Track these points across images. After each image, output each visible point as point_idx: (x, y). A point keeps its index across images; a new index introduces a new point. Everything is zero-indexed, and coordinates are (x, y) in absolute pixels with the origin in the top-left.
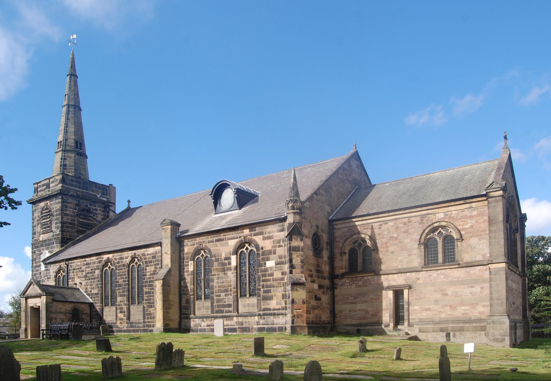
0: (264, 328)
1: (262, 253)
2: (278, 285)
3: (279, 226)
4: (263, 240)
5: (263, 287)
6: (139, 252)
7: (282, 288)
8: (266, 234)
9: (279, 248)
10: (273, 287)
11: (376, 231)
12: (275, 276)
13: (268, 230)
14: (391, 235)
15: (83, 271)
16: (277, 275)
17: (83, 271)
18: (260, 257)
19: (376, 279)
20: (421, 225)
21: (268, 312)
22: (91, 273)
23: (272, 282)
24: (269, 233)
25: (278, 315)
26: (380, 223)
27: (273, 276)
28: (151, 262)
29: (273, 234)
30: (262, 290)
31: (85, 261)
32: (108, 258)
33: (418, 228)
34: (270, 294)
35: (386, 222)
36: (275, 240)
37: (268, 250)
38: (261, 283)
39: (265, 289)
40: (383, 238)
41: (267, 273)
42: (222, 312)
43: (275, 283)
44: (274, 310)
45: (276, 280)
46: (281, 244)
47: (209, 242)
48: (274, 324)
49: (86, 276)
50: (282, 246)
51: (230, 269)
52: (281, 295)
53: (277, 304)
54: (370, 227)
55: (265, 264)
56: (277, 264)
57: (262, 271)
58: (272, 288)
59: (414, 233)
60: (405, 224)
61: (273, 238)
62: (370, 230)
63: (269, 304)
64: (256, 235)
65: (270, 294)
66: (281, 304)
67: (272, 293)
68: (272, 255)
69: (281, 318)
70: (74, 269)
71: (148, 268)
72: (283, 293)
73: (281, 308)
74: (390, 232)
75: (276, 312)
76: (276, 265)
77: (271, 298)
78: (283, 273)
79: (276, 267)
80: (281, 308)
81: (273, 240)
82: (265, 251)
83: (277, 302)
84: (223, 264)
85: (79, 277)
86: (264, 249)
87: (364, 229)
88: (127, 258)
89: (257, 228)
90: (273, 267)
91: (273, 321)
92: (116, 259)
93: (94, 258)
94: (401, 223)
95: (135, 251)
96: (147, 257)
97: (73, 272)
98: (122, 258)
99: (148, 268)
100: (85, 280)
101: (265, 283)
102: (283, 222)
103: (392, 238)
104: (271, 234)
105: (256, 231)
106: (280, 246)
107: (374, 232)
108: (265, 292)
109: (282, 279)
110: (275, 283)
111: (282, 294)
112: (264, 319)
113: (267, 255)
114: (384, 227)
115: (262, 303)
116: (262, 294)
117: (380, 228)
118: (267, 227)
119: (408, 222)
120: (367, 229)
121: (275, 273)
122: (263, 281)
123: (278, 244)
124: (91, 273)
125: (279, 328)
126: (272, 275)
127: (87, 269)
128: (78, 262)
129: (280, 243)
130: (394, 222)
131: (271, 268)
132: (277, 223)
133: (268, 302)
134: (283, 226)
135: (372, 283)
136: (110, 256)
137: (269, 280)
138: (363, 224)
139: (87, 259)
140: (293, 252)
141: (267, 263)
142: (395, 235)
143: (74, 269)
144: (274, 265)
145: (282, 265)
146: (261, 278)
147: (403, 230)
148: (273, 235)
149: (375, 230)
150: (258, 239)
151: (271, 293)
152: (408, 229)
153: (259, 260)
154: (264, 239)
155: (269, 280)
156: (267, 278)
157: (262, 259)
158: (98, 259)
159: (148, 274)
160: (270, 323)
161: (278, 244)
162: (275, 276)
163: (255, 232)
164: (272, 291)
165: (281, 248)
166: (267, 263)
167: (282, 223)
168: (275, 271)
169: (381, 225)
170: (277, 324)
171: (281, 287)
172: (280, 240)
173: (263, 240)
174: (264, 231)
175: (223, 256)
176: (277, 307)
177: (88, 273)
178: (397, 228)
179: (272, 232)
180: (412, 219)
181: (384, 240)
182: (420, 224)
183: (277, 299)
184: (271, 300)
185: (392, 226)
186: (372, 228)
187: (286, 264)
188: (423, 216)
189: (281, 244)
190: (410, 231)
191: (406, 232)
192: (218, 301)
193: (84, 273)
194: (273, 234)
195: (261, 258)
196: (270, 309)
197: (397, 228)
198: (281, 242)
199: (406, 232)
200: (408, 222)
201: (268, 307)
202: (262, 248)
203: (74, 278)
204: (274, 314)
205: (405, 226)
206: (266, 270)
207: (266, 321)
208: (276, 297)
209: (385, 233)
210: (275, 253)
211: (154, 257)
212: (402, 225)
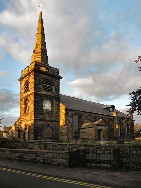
6: (108, 117)
15: (88, 118)
16: (130, 129)
17: (88, 118)
22: (91, 119)
28: (111, 121)
31: (89, 114)
32: (98, 116)
42: (122, 135)
47: (121, 119)
49: (89, 120)
51: (124, 126)
64: (128, 120)
70: (83, 116)
71: (110, 122)
84: (123, 125)
85: (86, 119)
88: (104, 118)
92: (101, 117)
93: (93, 114)
95: (107, 116)
96: (110, 119)
97: (83, 117)
98: (103, 117)
99: (110, 122)
100: (89, 121)
124: (91, 119)
127: (90, 117)
128: (86, 114)
136: (99, 115)
139: (90, 114)
143: (83, 116)
150: (128, 121)
158: (94, 115)
159: (110, 123)
175: (123, 123)
177: (90, 119)
192: (122, 132)
193: (88, 118)
203: (83, 119)
211: (112, 120)
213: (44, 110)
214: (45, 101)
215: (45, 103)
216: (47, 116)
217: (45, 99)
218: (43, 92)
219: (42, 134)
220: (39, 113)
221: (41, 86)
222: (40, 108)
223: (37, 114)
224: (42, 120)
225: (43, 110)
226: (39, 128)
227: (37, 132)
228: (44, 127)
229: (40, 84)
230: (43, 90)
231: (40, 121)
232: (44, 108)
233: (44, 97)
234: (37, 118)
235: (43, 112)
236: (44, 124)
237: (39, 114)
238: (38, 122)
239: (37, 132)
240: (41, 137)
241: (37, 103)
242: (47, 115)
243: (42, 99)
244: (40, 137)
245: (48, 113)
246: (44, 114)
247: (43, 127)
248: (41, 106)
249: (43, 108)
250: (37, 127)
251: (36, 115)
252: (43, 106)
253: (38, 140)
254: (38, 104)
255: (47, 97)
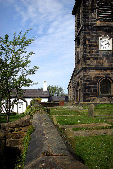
213: (99, 52)
214: (100, 36)
215: (101, 41)
216: (105, 61)
217: (101, 33)
218: (98, 23)
219: (96, 91)
220: (92, 58)
221: (95, 14)
222: (93, 49)
223: (89, 59)
224: (96, 69)
225: (98, 52)
226: (92, 81)
227: (88, 88)
228: (100, 79)
229: (93, 12)
230: (97, 20)
231: (93, 70)
232: (101, 48)
233: (100, 30)
234: (89, 65)
235: (98, 55)
236: (99, 74)
237: (92, 59)
238: (90, 71)
239: (88, 88)
240: (94, 96)
241: (89, 42)
242: (104, 60)
243: (97, 34)
244: (93, 96)
245: (107, 56)
246: (101, 58)
247: (98, 80)
248: (95, 46)
249: (98, 48)
250: (88, 81)
251: (87, 61)
252: (98, 45)
253: (89, 101)
254: (90, 44)
255: (105, 31)
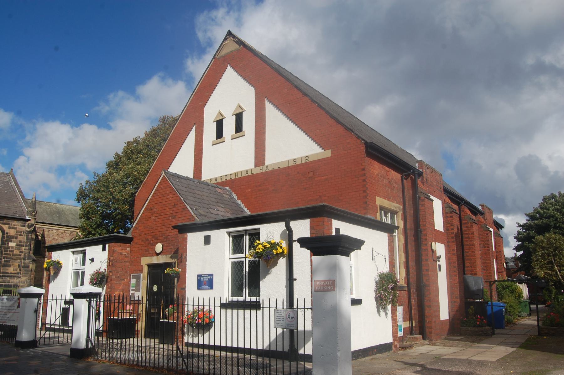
0: (3, 284)
1: (6, 237)
2: (16, 258)
3: (22, 223)
4: (9, 228)
5: (4, 258)
7: (19, 261)
8: (11, 225)
9: (20, 236)
10: (12, 259)
11: (46, 233)
12: (14, 253)
13: (14, 223)
14: (54, 237)
18: (4, 239)
19: (43, 259)
20: (70, 236)
21: (7, 275)
23: (12, 256)
24: (14, 225)
25: (14, 277)
26: (49, 229)
27: (13, 252)
29: (17, 226)
30: (3, 260)
33: (68, 237)
34: (9, 263)
35: (52, 230)
36: (18, 231)
37: (11, 236)
38: (3, 255)
39: (6, 260)
40: (49, 238)
41: (9, 250)
43: (14, 257)
44: (11, 273)
45: (16, 255)
46: (22, 234)
48: (9, 283)
50: (23, 236)
52: (18, 265)
53: (14, 270)
54: (43, 230)
55: (8, 244)
56: (17, 245)
57: (5, 248)
58: (11, 260)
59: (66, 239)
60: (62, 233)
61: (16, 229)
62: (42, 231)
63: (7, 270)
65: (9, 263)
66: (16, 271)
67: (11, 263)
68: (14, 239)
69: (15, 279)
72: (19, 264)
73: (16, 273)
74: (53, 235)
75: (13, 275)
76: (16, 246)
77: (10, 266)
78: (21, 252)
79: (16, 247)
80: (16, 273)
81: (16, 230)
82: (10, 236)
83: (14, 269)
86: (8, 235)
87: (39, 230)
89: (5, 220)
90: (14, 247)
91: (10, 281)
94: (60, 232)
101: (6, 256)
102: (25, 221)
103: (54, 239)
104: (15, 226)
105: (4, 221)
106: (21, 235)
107: (44, 233)
108: (5, 261)
109: (20, 255)
110: (14, 257)
111: (18, 265)
112: (2, 278)
113: (11, 238)
114: (51, 232)
115: (2, 268)
116: (3, 262)
117: (49, 232)
118: (13, 221)
119: (64, 233)
120: (41, 230)
121: (15, 251)
122: (5, 254)
123: (20, 234)
125: (14, 285)
126: (13, 251)
129: (21, 233)
130: (57, 231)
131: (12, 247)
132: (21, 221)
133: (7, 268)
134: (25, 223)
135: (40, 261)
137: (10, 255)
138: (39, 227)
140: (32, 241)
141: (10, 243)
142: (56, 238)
144: (15, 246)
145: (21, 247)
146: (4, 253)
147: (61, 236)
148: (16, 227)
149: (45, 232)
151: (10, 262)
152: (63, 236)
153: (4, 240)
154: (10, 228)
155: (10, 255)
156: (8, 253)
157: (6, 240)
160: (6, 281)
161: (20, 234)
162: (14, 253)
163: (3, 222)
164: (11, 261)
165: (22, 236)
166: (10, 243)
167: (24, 222)
168: (16, 249)
169: (49, 230)
170: (12, 283)
171: (18, 260)
172: (21, 232)
173: (9, 228)
174: (10, 223)
176: (14, 272)
178: (58, 234)
179: (17, 225)
180: (66, 231)
181: (50, 239)
182: (69, 235)
183: (14, 267)
184: (9, 267)
185: (55, 233)
186: (44, 231)
187: (24, 247)
188: (71, 232)
189: (22, 234)
190: (64, 237)
191: (62, 237)
194: (17, 226)
195: (5, 239)
196: (8, 273)
197: (58, 234)
198: (22, 233)
199: (62, 237)
200: (64, 233)
201: (7, 271)
202: (7, 233)
204: (11, 277)
205: (62, 234)
206: (9, 248)
207: (4, 280)
208: (13, 266)
209: (51, 235)
210: (16, 238)
212: (60, 233)
